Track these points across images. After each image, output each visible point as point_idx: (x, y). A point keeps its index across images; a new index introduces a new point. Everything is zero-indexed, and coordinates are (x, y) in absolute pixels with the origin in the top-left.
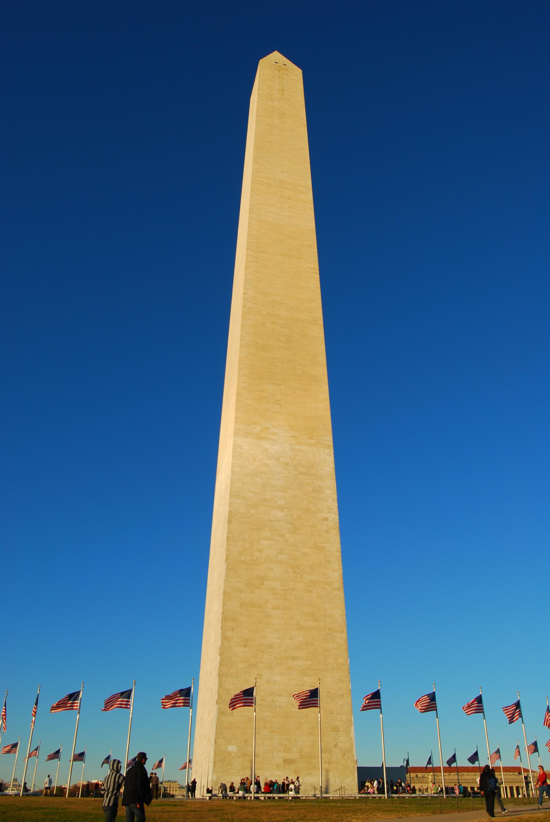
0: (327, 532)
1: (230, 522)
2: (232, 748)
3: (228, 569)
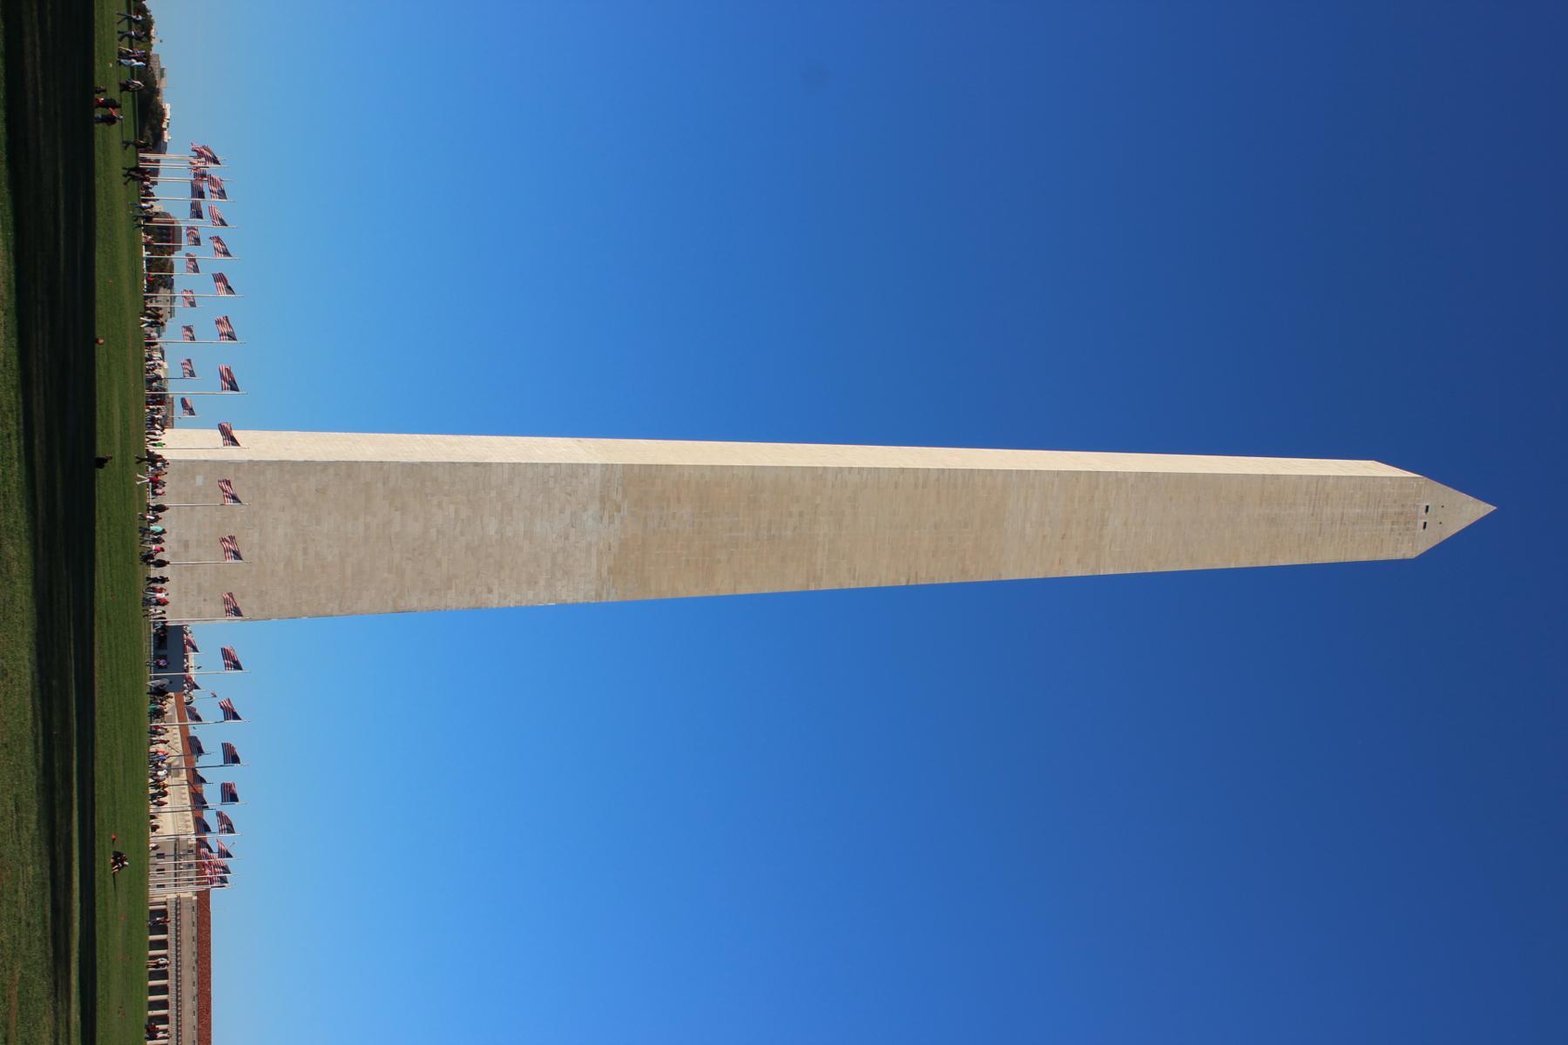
0: (473, 592)
1: (476, 464)
2: (199, 480)
3: (413, 465)
